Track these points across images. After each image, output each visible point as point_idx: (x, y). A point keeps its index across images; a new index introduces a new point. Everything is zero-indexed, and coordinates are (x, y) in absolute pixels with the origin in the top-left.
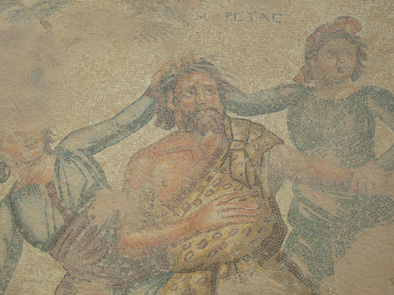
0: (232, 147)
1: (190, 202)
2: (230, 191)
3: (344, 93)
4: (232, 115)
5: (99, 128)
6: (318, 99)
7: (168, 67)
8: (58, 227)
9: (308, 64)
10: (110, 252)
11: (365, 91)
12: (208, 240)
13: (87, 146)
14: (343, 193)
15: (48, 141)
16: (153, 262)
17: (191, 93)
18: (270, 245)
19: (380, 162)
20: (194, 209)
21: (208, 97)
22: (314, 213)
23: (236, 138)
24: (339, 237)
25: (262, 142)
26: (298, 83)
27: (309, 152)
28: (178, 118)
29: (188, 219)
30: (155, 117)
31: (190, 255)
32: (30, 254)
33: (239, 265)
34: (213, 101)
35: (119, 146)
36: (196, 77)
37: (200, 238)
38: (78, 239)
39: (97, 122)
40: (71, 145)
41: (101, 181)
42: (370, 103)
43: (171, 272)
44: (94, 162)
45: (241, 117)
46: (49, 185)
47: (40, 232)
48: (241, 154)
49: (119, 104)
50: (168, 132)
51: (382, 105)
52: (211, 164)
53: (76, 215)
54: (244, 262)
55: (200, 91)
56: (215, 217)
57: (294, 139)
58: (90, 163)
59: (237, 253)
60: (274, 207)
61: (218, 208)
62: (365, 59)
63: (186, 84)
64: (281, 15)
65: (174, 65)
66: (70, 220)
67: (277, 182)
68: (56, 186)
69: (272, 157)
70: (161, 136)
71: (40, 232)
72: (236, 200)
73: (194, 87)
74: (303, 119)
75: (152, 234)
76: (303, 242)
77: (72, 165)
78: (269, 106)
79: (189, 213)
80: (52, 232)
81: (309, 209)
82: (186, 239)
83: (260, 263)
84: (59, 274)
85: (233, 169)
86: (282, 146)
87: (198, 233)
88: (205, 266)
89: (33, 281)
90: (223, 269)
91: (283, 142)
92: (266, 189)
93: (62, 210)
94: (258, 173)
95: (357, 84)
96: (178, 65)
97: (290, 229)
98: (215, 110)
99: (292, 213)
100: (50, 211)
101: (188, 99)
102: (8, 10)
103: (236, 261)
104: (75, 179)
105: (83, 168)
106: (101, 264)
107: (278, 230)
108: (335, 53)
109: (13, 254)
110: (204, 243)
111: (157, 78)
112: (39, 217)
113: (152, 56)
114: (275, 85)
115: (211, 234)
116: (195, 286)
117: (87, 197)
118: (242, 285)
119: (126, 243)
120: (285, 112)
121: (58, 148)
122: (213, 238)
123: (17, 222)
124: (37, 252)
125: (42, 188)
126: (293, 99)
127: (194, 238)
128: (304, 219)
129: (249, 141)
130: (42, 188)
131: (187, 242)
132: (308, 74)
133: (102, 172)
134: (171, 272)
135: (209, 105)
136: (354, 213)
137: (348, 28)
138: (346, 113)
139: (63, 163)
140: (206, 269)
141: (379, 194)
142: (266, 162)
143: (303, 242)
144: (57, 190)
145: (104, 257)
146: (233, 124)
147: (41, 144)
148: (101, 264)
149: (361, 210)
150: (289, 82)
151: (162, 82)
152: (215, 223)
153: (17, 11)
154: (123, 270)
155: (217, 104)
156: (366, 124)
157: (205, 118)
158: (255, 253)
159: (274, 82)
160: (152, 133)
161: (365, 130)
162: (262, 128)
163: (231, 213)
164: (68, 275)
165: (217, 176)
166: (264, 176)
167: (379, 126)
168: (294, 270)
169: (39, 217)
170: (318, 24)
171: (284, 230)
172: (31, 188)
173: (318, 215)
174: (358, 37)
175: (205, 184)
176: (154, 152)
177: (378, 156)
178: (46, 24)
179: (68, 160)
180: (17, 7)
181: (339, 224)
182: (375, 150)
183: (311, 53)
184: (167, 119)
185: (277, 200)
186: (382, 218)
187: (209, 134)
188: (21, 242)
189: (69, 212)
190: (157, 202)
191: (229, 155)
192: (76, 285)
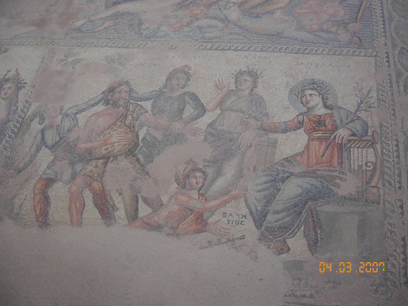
0: (128, 113)
1: (106, 133)
2: (123, 130)
3: (178, 94)
4: (131, 101)
5: (81, 106)
6: (166, 96)
7: (113, 83)
8: (56, 141)
9: (166, 83)
10: (72, 151)
11: (185, 93)
12: (109, 148)
13: (75, 112)
14: (166, 132)
15: (62, 110)
16: (87, 155)
17: (119, 93)
18: (131, 152)
19: (184, 120)
20: (107, 136)
21: (125, 95)
22: (152, 139)
23: (130, 110)
24: (159, 149)
25: (140, 112)
26: (160, 90)
27: (157, 116)
28: (111, 102)
29: (104, 139)
30: (103, 102)
31: (101, 153)
32: (45, 151)
33: (118, 158)
34: (126, 96)
35: (86, 112)
36: (122, 87)
37: (106, 147)
38: (62, 145)
39: (81, 103)
40: (69, 112)
41: (76, 125)
42: (187, 98)
43: (92, 159)
44: (76, 118)
45: (135, 102)
46: (58, 126)
47: (50, 142)
48: (131, 116)
49: (91, 97)
50: (106, 107)
51: (191, 99)
52: (118, 119)
53: (64, 137)
54: (120, 156)
55: (122, 92)
56: (114, 139)
57: (152, 111)
58: (74, 118)
59: (118, 153)
60: (137, 136)
61: (116, 136)
62: (189, 81)
63: (118, 90)
64: (161, 64)
65: (116, 83)
66: (61, 139)
67: (141, 126)
68: (60, 126)
69: (142, 118)
70: (103, 109)
71: (50, 142)
72: (124, 133)
73: (121, 91)
74: (158, 103)
75: (89, 145)
76: (145, 150)
77: (68, 119)
78: (147, 98)
79: (105, 138)
80: (54, 143)
81: (151, 137)
82: (101, 147)
83: (126, 157)
84: (52, 158)
85: (126, 121)
86: (147, 114)
87: (106, 145)
88: (105, 158)
89: (42, 160)
90: (111, 159)
91: (148, 112)
92: (136, 129)
93: (59, 135)
94: (135, 123)
95: (183, 90)
96: (117, 82)
97: (141, 145)
98: (126, 99)
99: (143, 139)
100: (55, 135)
101: (117, 95)
102: (62, 63)
103: (117, 156)
104: (67, 124)
105: (71, 120)
106: (68, 155)
107: (137, 145)
108: (178, 79)
109: (38, 150)
110: (107, 149)
111: (108, 88)
112: (51, 137)
113: (109, 79)
114: (151, 91)
115: (110, 146)
116: (99, 165)
117: (69, 130)
118: (117, 165)
119: (79, 148)
120: (152, 101)
121: (65, 113)
122: (111, 147)
123: (43, 139)
124: (47, 150)
125: (55, 127)
126: (157, 96)
127: (104, 147)
128: (148, 141)
129: (135, 111)
130: (55, 127)
131: (101, 148)
132: (165, 86)
133: (78, 121)
134: (92, 159)
135: (124, 98)
136: (167, 139)
137: (186, 69)
138: (176, 101)
139: (65, 118)
140: (105, 159)
141: (180, 132)
142: (139, 119)
143: (145, 150)
144: (60, 128)
145: (70, 153)
146: (131, 105)
147: (59, 111)
148: (68, 155)
149: (171, 138)
150: (157, 89)
151: (109, 89)
152: (113, 142)
153: (66, 63)
154: (75, 157)
155: (127, 98)
156: (182, 106)
157: (121, 102)
158: (125, 153)
159: (151, 89)
160: (101, 108)
161: (181, 108)
162: (141, 106)
163: (120, 138)
164: (55, 158)
165: (119, 124)
166: (136, 125)
167: (188, 106)
168: (138, 160)
169: (51, 137)
170: (175, 68)
171: (139, 145)
172: (51, 127)
173: (153, 140)
174: (189, 73)
175: (114, 126)
176: (98, 115)
177: (183, 118)
178: (74, 68)
179: (66, 117)
180: (66, 62)
181: (160, 143)
182: (183, 116)
183: (169, 79)
184: (107, 102)
185: (139, 134)
186: (178, 141)
187: (121, 108)
188: (42, 146)
189: (62, 136)
190: (94, 133)
191: (126, 116)
192: (56, 162)
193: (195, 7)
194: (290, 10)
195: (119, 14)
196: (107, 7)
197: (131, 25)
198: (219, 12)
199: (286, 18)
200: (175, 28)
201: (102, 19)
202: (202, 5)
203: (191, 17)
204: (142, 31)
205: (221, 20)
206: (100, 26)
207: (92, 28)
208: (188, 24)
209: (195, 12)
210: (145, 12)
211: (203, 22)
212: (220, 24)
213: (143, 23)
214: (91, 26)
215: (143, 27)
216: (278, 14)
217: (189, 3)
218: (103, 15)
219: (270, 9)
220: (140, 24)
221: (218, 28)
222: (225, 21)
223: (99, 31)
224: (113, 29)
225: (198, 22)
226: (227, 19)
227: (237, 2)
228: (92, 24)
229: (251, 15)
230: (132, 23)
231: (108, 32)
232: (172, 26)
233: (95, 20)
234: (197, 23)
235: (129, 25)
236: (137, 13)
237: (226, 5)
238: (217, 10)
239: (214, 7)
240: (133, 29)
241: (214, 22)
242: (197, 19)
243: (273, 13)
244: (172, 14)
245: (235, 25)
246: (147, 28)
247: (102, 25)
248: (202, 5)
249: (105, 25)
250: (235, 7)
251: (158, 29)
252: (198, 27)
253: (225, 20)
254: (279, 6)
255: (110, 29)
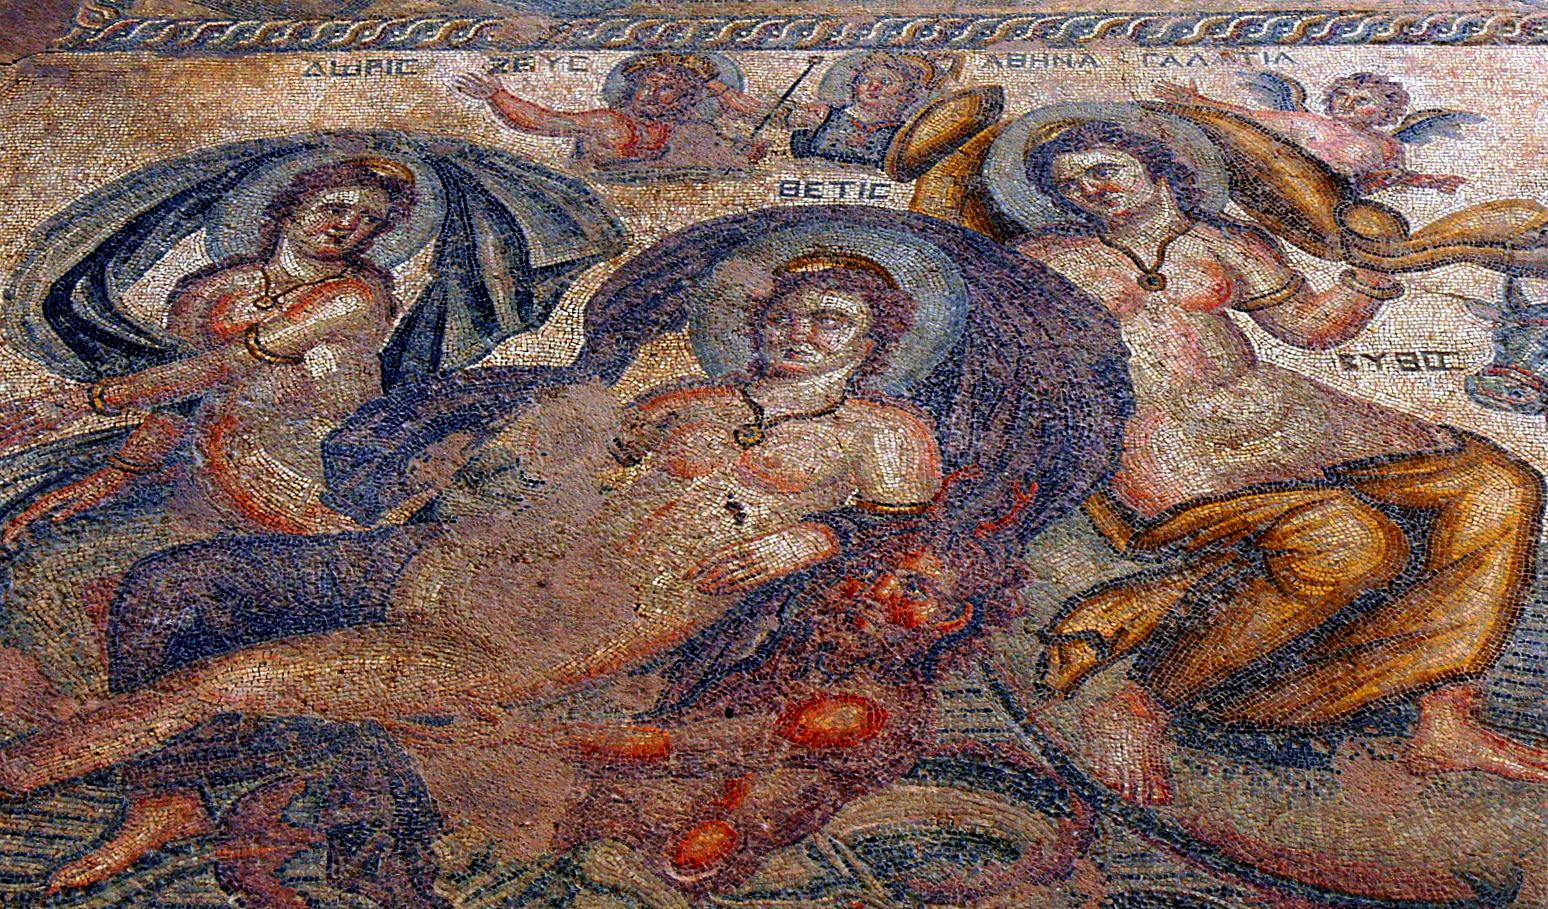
193: (815, 677)
194: (1523, 692)
195: (231, 738)
196: (129, 678)
197: (342, 839)
198: (1002, 718)
199: (1514, 766)
200: (696, 865)
201: (100, 777)
202: (859, 660)
203: (794, 762)
204: (438, 891)
205: (1027, 785)
206: (96, 844)
207: (37, 857)
208: (792, 831)
209: (826, 721)
210: (440, 722)
211: (901, 808)
212: (1029, 823)
213: (440, 818)
214: (17, 844)
215: (443, 850)
216: (1443, 729)
217: (761, 647)
218: (108, 752)
219: (1375, 690)
220: (417, 824)
221: (1025, 860)
222: (1062, 794)
223: (92, 888)
224: (202, 871)
225: (852, 808)
226: (1075, 777)
227: (1121, 632)
228: (24, 825)
229: (1247, 740)
230: (341, 815)
231: (170, 895)
232: (670, 844)
233: (46, 791)
234: (856, 818)
235: (331, 837)
236: (374, 728)
237: (1044, 663)
238: (979, 702)
239: (952, 680)
240: (367, 868)
241: (984, 809)
242: (850, 785)
243: (1401, 721)
244: (646, 738)
245: (1145, 824)
246: (474, 867)
247: (111, 832)
248: (859, 660)
249: (139, 839)
250: (1113, 679)
251: (561, 868)
252: (867, 846)
253: (1062, 786)
254: (1435, 661)
255: (179, 874)
